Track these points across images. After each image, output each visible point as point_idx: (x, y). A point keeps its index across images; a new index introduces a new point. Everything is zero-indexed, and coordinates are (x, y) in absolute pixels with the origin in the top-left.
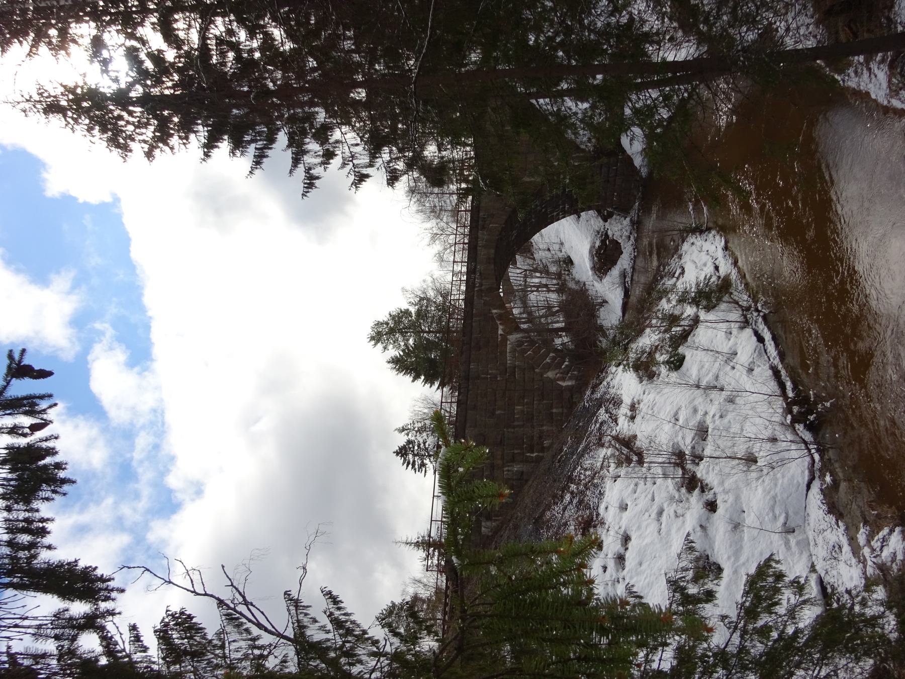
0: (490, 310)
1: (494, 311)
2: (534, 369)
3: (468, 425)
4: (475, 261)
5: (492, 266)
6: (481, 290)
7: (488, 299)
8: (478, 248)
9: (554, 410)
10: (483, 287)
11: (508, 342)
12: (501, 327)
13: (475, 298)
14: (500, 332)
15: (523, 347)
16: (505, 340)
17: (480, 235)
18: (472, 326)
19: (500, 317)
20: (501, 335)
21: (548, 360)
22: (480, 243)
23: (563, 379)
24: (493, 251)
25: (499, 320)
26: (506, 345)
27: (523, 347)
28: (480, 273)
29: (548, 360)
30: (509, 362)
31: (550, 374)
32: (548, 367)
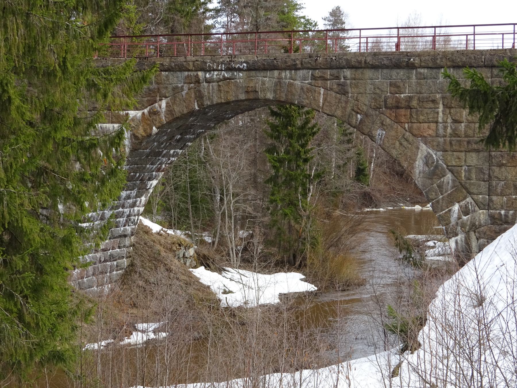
0: (166, 97)
1: (164, 103)
4: (249, 69)
5: (242, 97)
6: (198, 81)
7: (184, 93)
8: (276, 73)
12: (139, 114)
13: (186, 73)
14: (132, 113)
17: (301, 73)
19: (154, 113)
20: (127, 114)
24: (270, 96)
25: (149, 112)
26: (112, 123)
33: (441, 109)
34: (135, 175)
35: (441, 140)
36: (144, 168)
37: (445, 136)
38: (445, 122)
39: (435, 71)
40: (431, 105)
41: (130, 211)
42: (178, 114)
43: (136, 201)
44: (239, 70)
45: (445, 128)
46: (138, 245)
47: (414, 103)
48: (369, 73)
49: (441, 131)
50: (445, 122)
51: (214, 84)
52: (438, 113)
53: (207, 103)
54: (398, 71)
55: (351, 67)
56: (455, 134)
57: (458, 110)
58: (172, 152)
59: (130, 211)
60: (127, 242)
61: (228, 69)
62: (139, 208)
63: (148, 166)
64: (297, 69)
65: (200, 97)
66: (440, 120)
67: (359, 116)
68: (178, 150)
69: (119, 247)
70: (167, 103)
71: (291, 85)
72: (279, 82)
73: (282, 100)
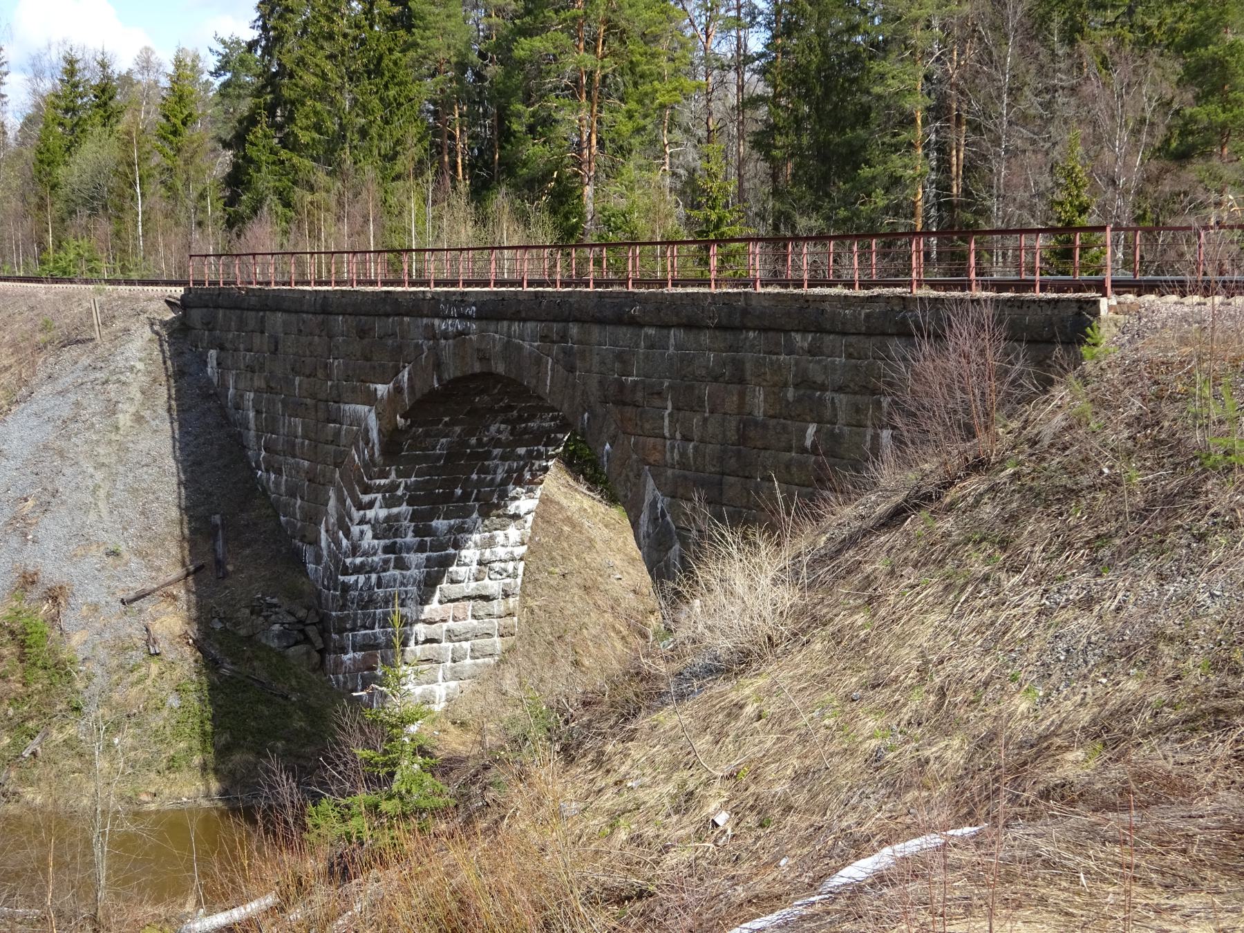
1: (405, 375)
2: (336, 465)
3: (285, 316)
4: (480, 317)
5: (477, 368)
6: (434, 337)
8: (505, 323)
9: (299, 502)
10: (443, 341)
11: (367, 408)
14: (382, 389)
15: (361, 443)
16: (370, 399)
17: (530, 325)
18: (388, 315)
21: (349, 501)
22: (516, 327)
23: (327, 531)
27: (361, 443)
28: (460, 334)
29: (349, 501)
30: (347, 407)
31: (332, 503)
32: (340, 500)
33: (668, 412)
34: (453, 492)
35: (670, 472)
36: (468, 479)
37: (673, 467)
38: (673, 438)
39: (665, 332)
40: (657, 402)
41: (482, 554)
42: (418, 395)
43: (492, 538)
44: (469, 318)
45: (673, 448)
46: (542, 613)
47: (639, 396)
48: (595, 332)
49: (668, 455)
50: (673, 438)
51: (451, 341)
52: (662, 418)
53: (446, 377)
54: (624, 329)
55: (576, 320)
56: (683, 465)
57: (687, 413)
58: (522, 451)
59: (482, 554)
60: (497, 607)
61: (462, 317)
62: (509, 549)
63: (474, 476)
64: (525, 320)
65: (438, 365)
66: (667, 435)
67: (586, 415)
68: (542, 449)
69: (474, 617)
70: (409, 374)
71: (520, 348)
72: (508, 345)
73: (513, 376)
